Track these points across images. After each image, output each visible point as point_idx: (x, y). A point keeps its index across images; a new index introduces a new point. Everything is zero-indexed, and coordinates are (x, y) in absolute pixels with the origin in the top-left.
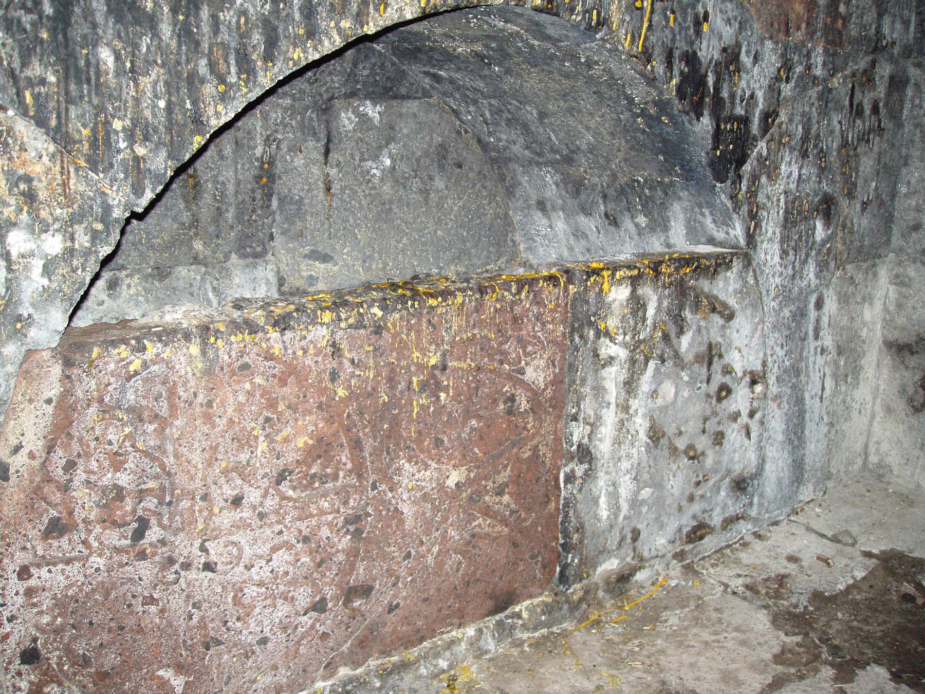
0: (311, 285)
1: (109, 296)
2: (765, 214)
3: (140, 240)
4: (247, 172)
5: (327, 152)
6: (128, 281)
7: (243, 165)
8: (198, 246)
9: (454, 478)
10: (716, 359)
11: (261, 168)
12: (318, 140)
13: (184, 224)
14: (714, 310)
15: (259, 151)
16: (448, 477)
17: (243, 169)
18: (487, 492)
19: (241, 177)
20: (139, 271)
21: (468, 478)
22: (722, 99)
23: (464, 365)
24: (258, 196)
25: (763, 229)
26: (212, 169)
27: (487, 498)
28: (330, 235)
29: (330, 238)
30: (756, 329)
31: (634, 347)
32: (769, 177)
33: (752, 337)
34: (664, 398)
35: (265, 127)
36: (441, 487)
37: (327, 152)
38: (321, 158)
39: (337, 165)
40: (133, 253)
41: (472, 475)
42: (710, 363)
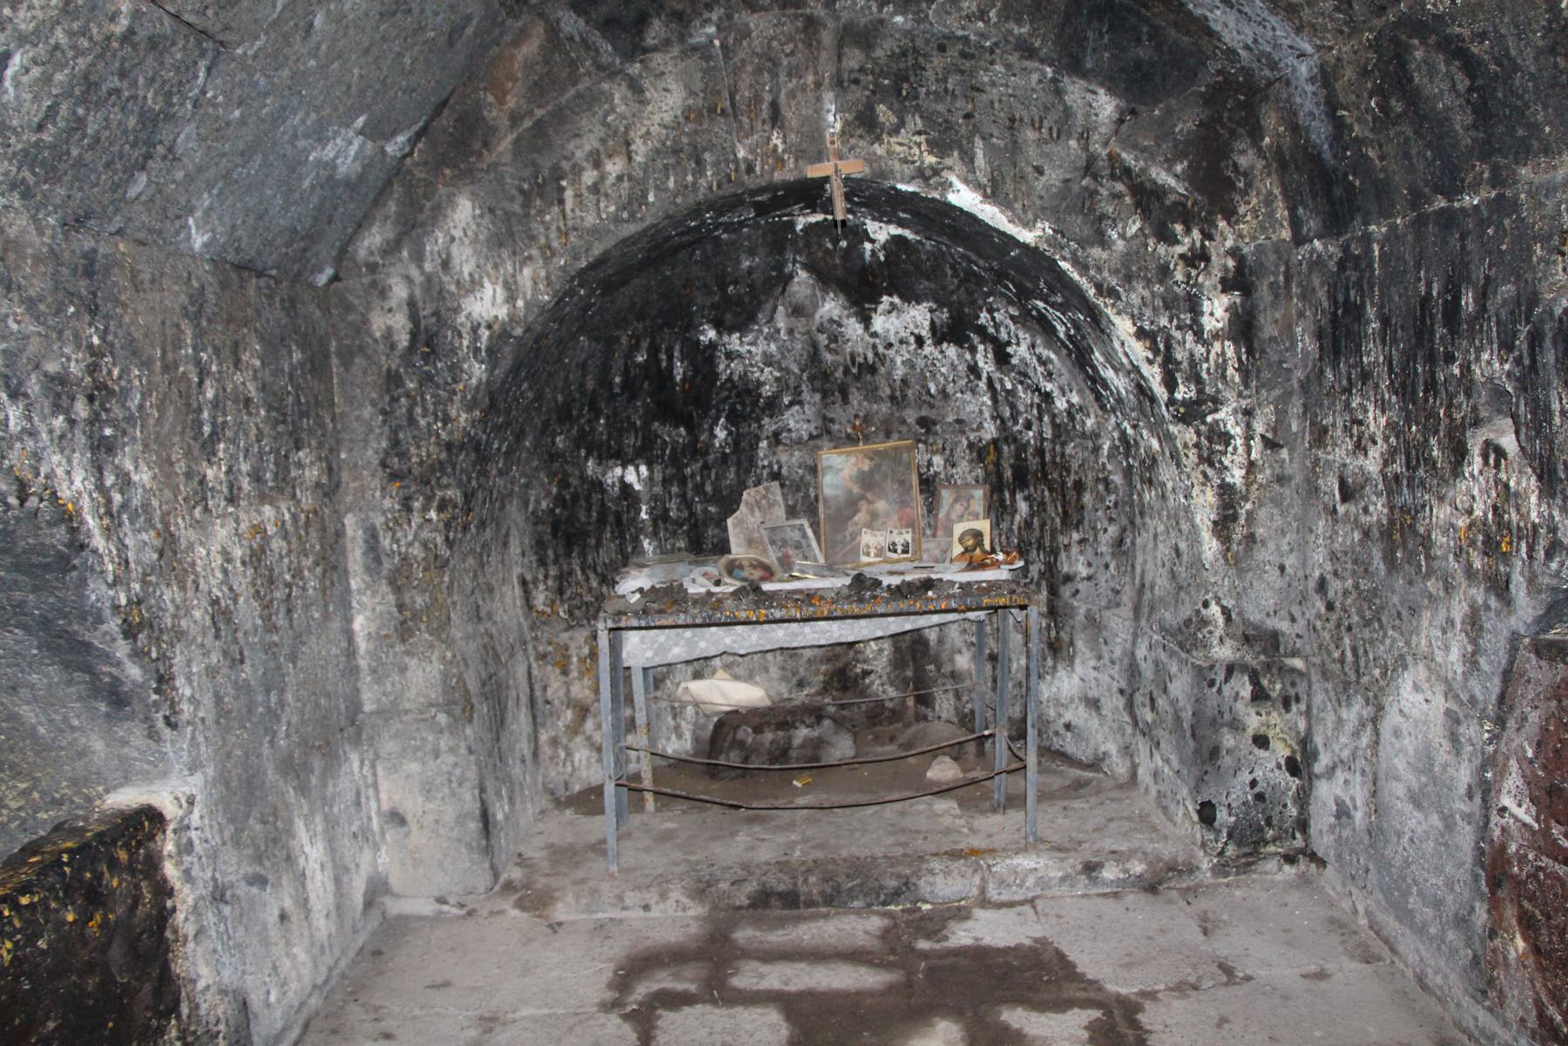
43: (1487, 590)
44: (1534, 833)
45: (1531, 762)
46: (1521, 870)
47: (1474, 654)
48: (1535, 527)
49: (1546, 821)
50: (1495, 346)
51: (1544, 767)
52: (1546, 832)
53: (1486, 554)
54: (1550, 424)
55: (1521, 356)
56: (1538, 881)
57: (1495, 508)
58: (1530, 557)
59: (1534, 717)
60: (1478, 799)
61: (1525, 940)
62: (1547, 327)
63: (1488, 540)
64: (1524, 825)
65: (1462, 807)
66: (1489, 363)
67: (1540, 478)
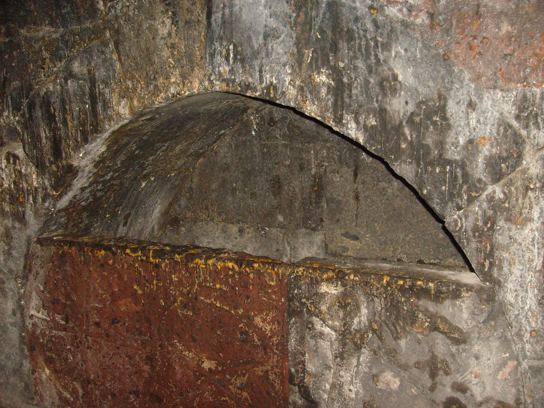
0: (344, 252)
1: (239, 235)
2: (505, 255)
3: (253, 211)
4: (307, 183)
5: (356, 175)
6: (248, 230)
7: (304, 178)
8: (280, 218)
9: (207, 365)
10: (441, 372)
11: (315, 181)
12: (349, 167)
13: (273, 206)
14: (434, 328)
15: (313, 171)
16: (203, 362)
17: (304, 180)
18: (231, 384)
19: (304, 185)
20: (252, 226)
21: (216, 367)
22: (428, 146)
23: (208, 301)
24: (313, 196)
25: (506, 269)
26: (287, 179)
27: (230, 387)
28: (356, 224)
29: (356, 225)
30: (504, 364)
31: (344, 334)
32: (508, 220)
33: (500, 369)
34: (388, 384)
35: (316, 158)
36: (199, 366)
37: (356, 175)
38: (352, 178)
39: (363, 183)
40: (250, 217)
41: (220, 369)
42: (433, 375)
43: (13, 220)
44: (48, 322)
45: (43, 292)
46: (44, 339)
47: (9, 250)
48: (36, 188)
49: (53, 315)
50: (11, 109)
51: (49, 293)
52: (53, 320)
53: (11, 203)
54: (41, 143)
55: (24, 114)
56: (53, 342)
57: (15, 183)
58: (35, 202)
59: (42, 272)
60: (18, 315)
61: (49, 369)
62: (37, 100)
63: (12, 197)
64: (43, 320)
65: (11, 320)
66: (7, 117)
67: (37, 167)
